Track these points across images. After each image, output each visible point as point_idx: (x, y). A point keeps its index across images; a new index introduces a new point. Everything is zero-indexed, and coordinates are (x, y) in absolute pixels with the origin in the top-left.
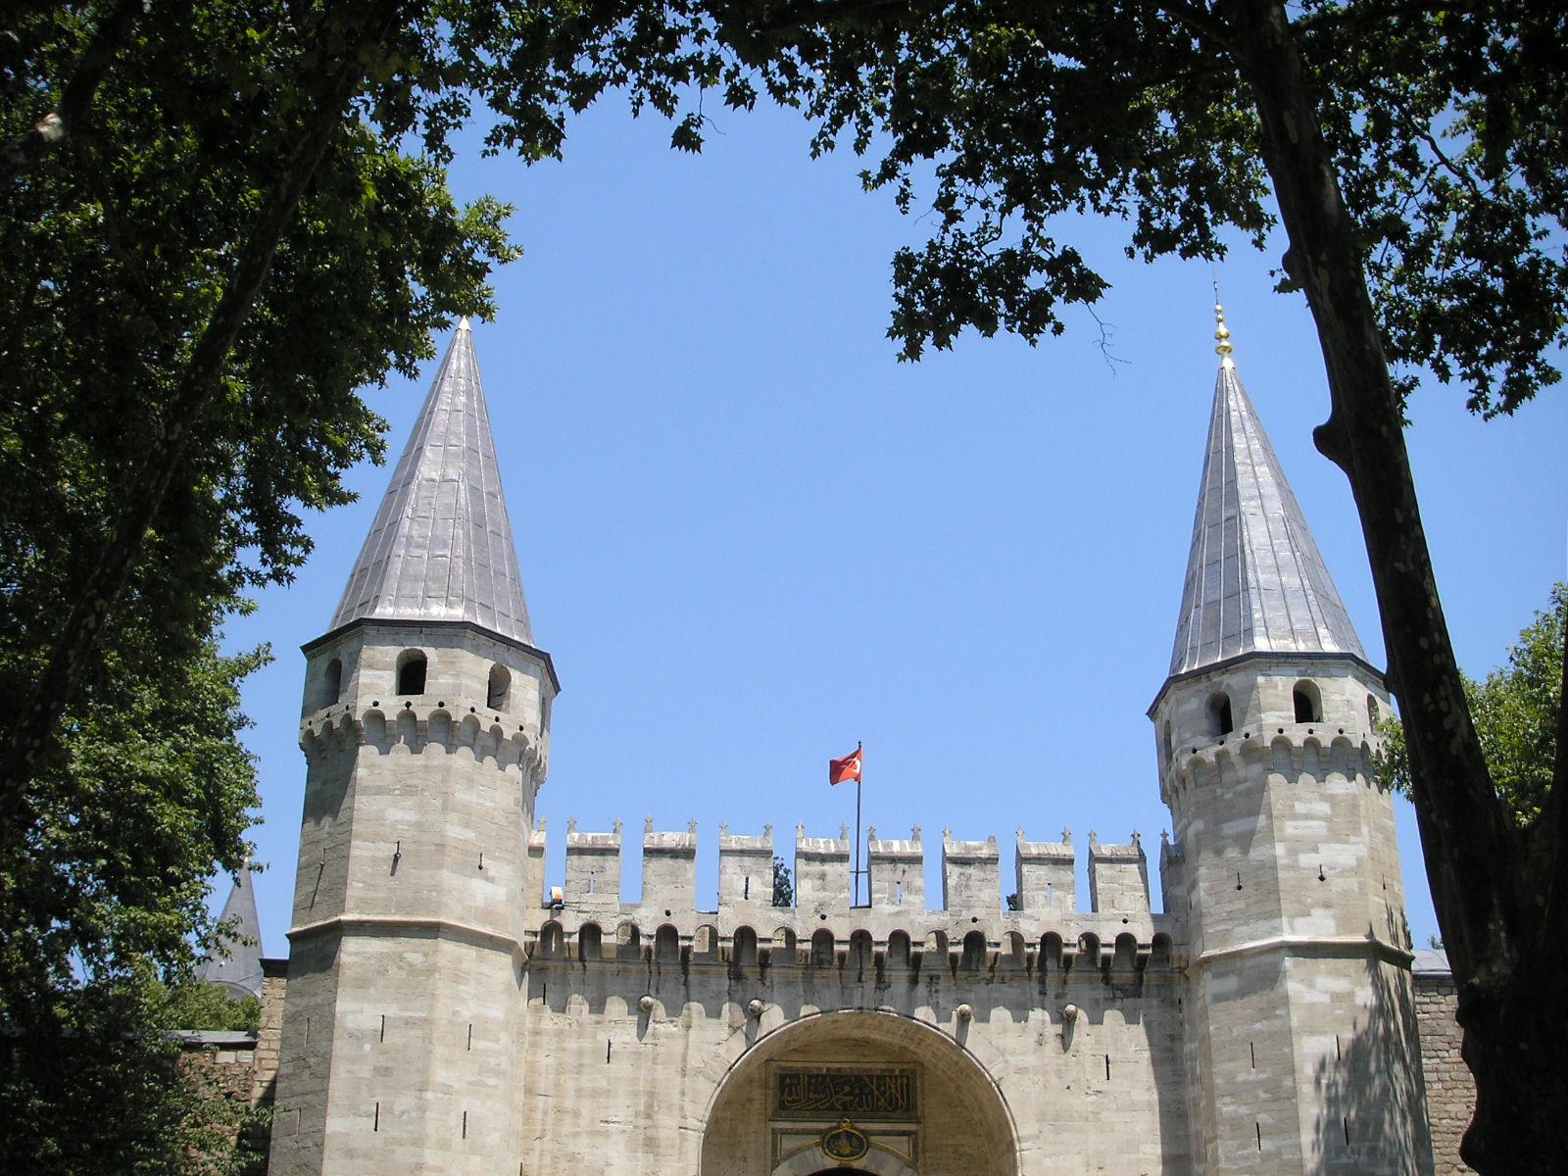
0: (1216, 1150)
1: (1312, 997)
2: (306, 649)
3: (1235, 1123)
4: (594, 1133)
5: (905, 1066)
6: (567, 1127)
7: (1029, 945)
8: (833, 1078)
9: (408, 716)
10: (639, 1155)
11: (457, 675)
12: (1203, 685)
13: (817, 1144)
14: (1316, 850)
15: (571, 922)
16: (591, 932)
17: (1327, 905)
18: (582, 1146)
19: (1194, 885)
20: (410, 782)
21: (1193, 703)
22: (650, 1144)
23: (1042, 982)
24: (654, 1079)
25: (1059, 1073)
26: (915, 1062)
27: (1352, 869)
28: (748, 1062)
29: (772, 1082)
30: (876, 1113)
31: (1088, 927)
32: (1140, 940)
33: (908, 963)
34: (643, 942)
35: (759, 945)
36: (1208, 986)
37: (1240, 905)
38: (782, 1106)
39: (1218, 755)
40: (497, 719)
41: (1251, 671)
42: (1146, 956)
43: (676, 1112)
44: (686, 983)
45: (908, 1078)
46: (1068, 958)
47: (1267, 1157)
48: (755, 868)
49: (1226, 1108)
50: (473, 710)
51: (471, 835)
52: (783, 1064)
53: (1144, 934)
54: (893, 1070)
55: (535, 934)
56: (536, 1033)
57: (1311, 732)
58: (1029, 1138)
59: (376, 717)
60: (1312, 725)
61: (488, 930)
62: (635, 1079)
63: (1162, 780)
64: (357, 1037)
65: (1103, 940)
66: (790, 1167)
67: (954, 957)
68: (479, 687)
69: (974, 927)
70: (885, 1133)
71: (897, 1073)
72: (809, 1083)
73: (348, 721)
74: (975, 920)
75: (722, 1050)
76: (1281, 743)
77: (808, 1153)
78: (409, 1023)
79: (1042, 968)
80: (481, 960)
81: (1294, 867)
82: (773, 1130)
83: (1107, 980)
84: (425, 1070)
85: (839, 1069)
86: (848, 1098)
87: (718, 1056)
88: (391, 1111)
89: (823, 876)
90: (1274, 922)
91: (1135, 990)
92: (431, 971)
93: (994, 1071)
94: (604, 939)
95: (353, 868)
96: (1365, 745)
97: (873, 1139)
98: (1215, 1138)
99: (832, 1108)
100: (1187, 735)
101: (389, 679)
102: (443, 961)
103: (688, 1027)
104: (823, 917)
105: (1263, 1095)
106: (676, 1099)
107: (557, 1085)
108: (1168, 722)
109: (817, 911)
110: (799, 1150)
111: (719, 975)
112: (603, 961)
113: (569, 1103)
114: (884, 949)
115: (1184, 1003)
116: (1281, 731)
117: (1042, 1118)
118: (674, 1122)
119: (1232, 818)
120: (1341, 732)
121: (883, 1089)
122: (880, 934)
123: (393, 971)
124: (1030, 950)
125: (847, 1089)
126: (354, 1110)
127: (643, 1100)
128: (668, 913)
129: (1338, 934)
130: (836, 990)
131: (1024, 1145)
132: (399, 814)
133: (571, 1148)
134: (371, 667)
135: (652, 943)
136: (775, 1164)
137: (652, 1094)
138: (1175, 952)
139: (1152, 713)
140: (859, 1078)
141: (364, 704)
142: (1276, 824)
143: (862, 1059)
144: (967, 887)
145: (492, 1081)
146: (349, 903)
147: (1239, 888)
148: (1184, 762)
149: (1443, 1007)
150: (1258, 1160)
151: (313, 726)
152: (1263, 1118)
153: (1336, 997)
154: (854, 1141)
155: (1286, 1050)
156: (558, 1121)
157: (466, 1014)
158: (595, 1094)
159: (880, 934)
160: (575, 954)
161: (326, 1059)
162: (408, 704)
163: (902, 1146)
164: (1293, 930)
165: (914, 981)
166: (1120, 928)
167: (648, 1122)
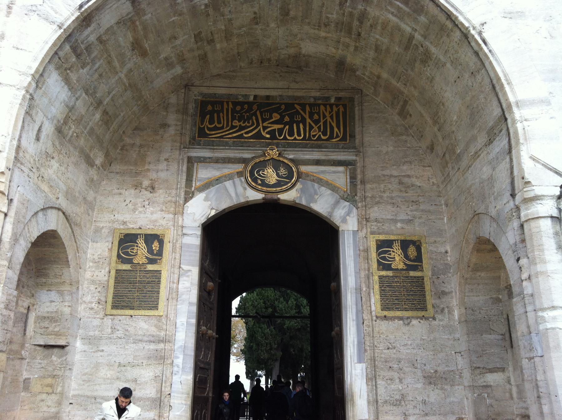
5: (342, 94)
8: (260, 106)
13: (240, 174)
26: (353, 88)
29: (191, 107)
30: (308, 143)
38: (202, 133)
45: (345, 106)
52: (205, 90)
54: (328, 98)
66: (206, 199)
70: (318, 163)
71: (333, 101)
72: (234, 111)
77: (228, 184)
85: (268, 97)
86: (276, 127)
97: (303, 168)
99: (258, 136)
110: (218, 180)
121: (316, 117)
125: (276, 116)
136: (189, 196)
140: (290, 106)
143: (293, 85)
154: (283, 171)
163: (339, 177)
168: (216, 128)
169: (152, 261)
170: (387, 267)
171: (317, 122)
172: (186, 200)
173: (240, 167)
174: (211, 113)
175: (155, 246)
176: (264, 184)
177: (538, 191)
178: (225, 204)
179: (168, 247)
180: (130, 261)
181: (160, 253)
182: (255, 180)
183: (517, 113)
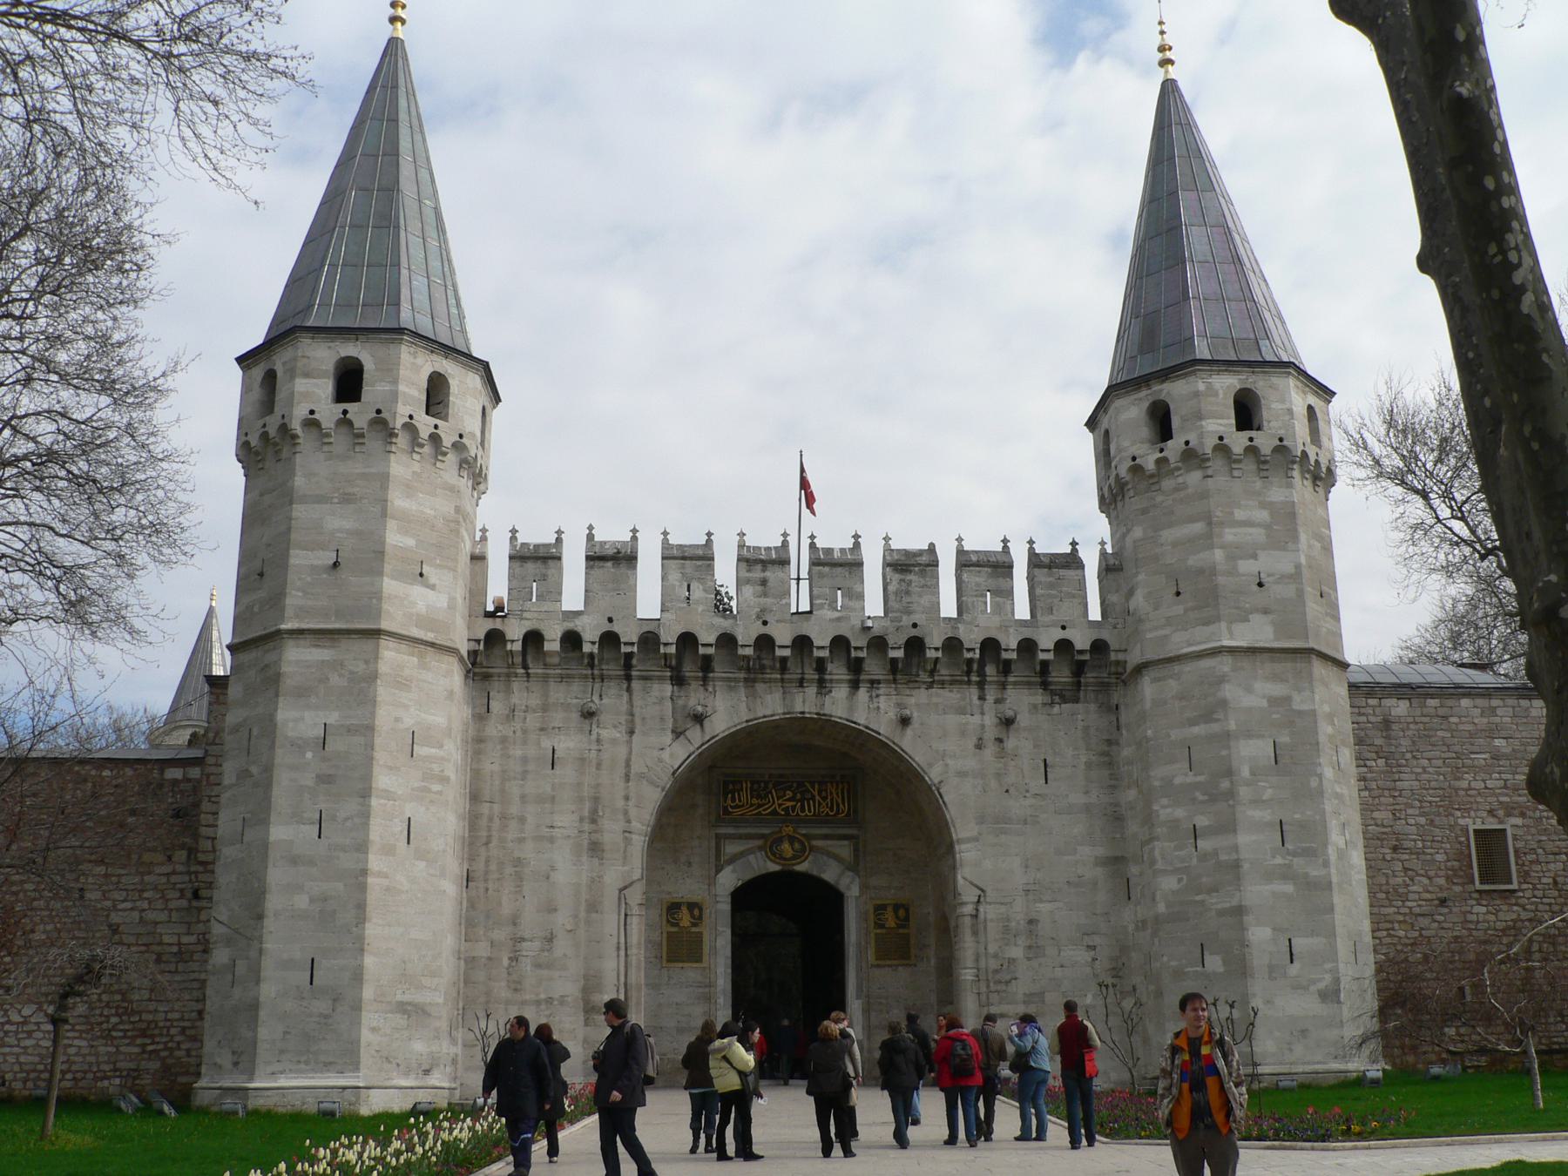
0: (1153, 849)
1: (1248, 701)
2: (240, 360)
3: (1174, 824)
4: (539, 838)
6: (512, 832)
7: (969, 650)
9: (345, 422)
10: (584, 859)
11: (395, 382)
12: (1144, 393)
13: (760, 848)
14: (1255, 557)
15: (515, 632)
16: (533, 639)
17: (1266, 612)
18: (528, 851)
19: (1131, 593)
20: (351, 490)
21: (1132, 411)
22: (595, 849)
23: (981, 685)
24: (598, 785)
25: (998, 776)
27: (1291, 576)
28: (691, 768)
31: (1027, 633)
32: (1078, 646)
33: (849, 669)
34: (587, 648)
35: (702, 651)
36: (1148, 688)
37: (1179, 609)
39: (1159, 462)
40: (436, 427)
41: (1192, 379)
42: (1085, 662)
43: (621, 817)
44: (629, 689)
46: (1008, 663)
47: (1204, 857)
48: (697, 574)
49: (1165, 811)
50: (411, 417)
51: (411, 542)
53: (1081, 641)
55: (478, 641)
56: (479, 740)
57: (1251, 439)
58: (969, 840)
59: (311, 423)
60: (1253, 434)
61: (430, 637)
62: (579, 784)
63: (1100, 489)
64: (299, 745)
65: (1042, 646)
66: (734, 871)
67: (894, 661)
68: (416, 393)
69: (914, 632)
73: (284, 429)
74: (915, 626)
75: (666, 755)
76: (1222, 448)
77: (751, 858)
78: (350, 730)
79: (982, 673)
80: (423, 666)
81: (1233, 572)
82: (718, 836)
83: (1045, 685)
84: (367, 778)
85: (781, 776)
87: (660, 760)
88: (333, 818)
89: (764, 582)
90: (1211, 628)
91: (1072, 694)
92: (373, 677)
93: (934, 775)
94: (547, 647)
95: (292, 576)
96: (1304, 453)
97: (814, 843)
98: (1152, 839)
100: (1126, 444)
101: (327, 387)
102: (383, 668)
103: (631, 732)
104: (765, 623)
105: (1201, 798)
106: (620, 803)
107: (503, 791)
108: (1107, 432)
109: (758, 617)
110: (742, 854)
111: (661, 679)
112: (546, 665)
113: (514, 810)
114: (825, 653)
115: (1122, 707)
116: (1221, 438)
117: (981, 820)
118: (619, 826)
119: (1170, 525)
120: (1281, 440)
122: (821, 639)
123: (335, 680)
124: (968, 655)
125: (789, 794)
126: (297, 817)
127: (587, 805)
128: (610, 620)
129: (1277, 639)
130: (778, 695)
131: (963, 847)
132: (338, 522)
133: (517, 854)
134: (307, 375)
135: (595, 649)
136: (718, 871)
137: (596, 800)
138: (1113, 656)
139: (1092, 423)
140: (801, 784)
141: (300, 412)
142: (1216, 530)
144: (908, 593)
145: (436, 787)
146: (289, 612)
147: (1178, 594)
148: (1123, 471)
149: (1372, 719)
150: (1195, 861)
151: (249, 438)
152: (1202, 821)
153: (1274, 702)
154: (797, 845)
155: (1224, 753)
156: (504, 827)
157: (408, 721)
158: (540, 799)
159: (821, 639)
160: (518, 660)
161: (268, 769)
162: (345, 412)
163: (844, 849)
164: (1232, 638)
165: (855, 685)
166: (1059, 634)
167: (593, 827)
168: (737, 807)
169: (694, 925)
170: (882, 926)
171: (824, 799)
172: (718, 872)
173: (760, 842)
174: (733, 793)
175: (696, 912)
176: (781, 858)
177: (965, 898)
178: (749, 876)
179: (706, 913)
180: (677, 925)
181: (700, 917)
182: (774, 854)
183: (957, 847)
